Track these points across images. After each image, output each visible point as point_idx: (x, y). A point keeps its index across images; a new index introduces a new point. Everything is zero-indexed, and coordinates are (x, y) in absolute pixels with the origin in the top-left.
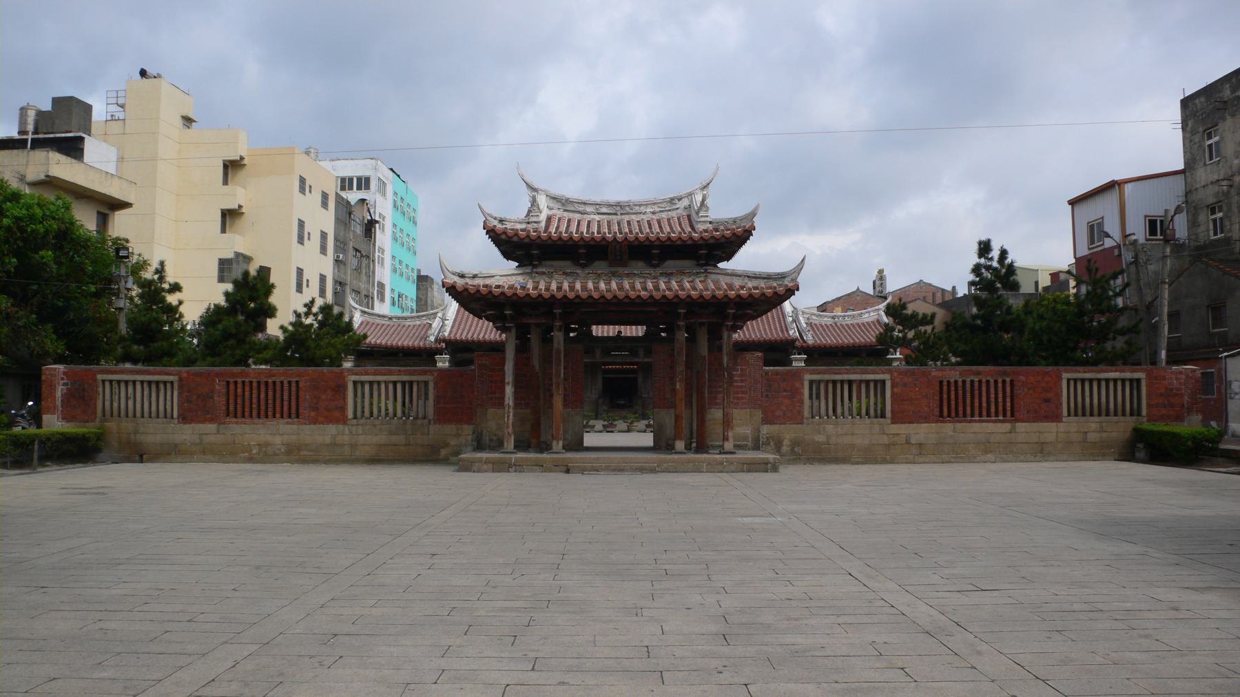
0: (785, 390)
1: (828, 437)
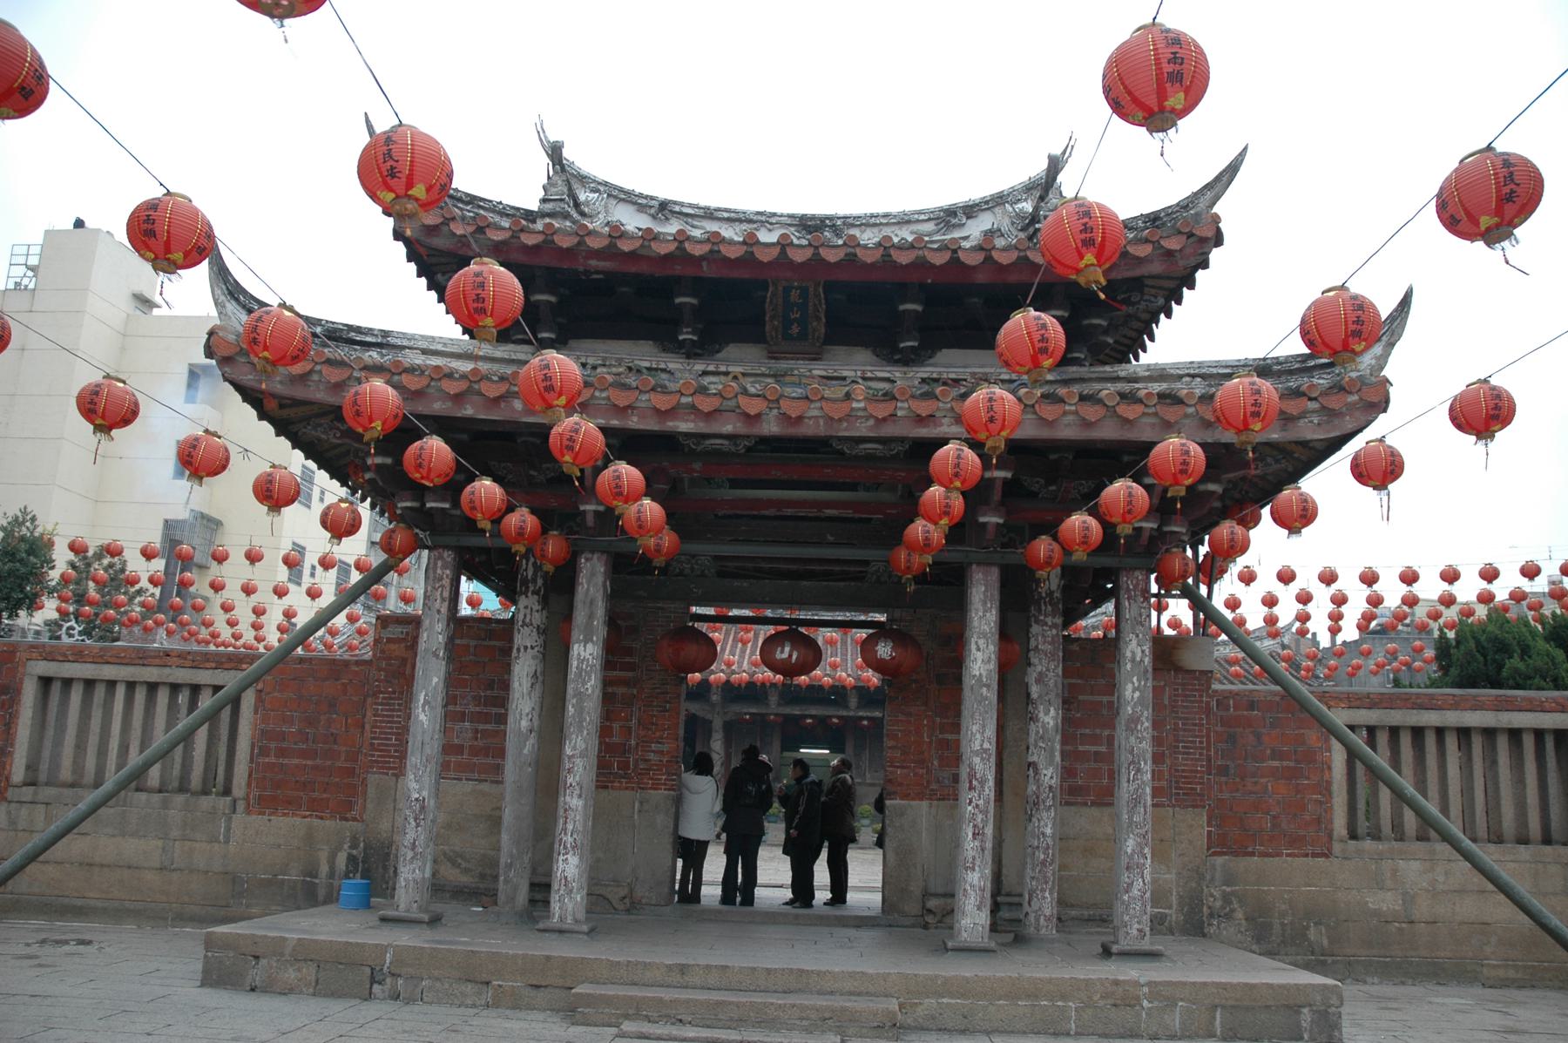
0: (1277, 755)
1: (1409, 899)
